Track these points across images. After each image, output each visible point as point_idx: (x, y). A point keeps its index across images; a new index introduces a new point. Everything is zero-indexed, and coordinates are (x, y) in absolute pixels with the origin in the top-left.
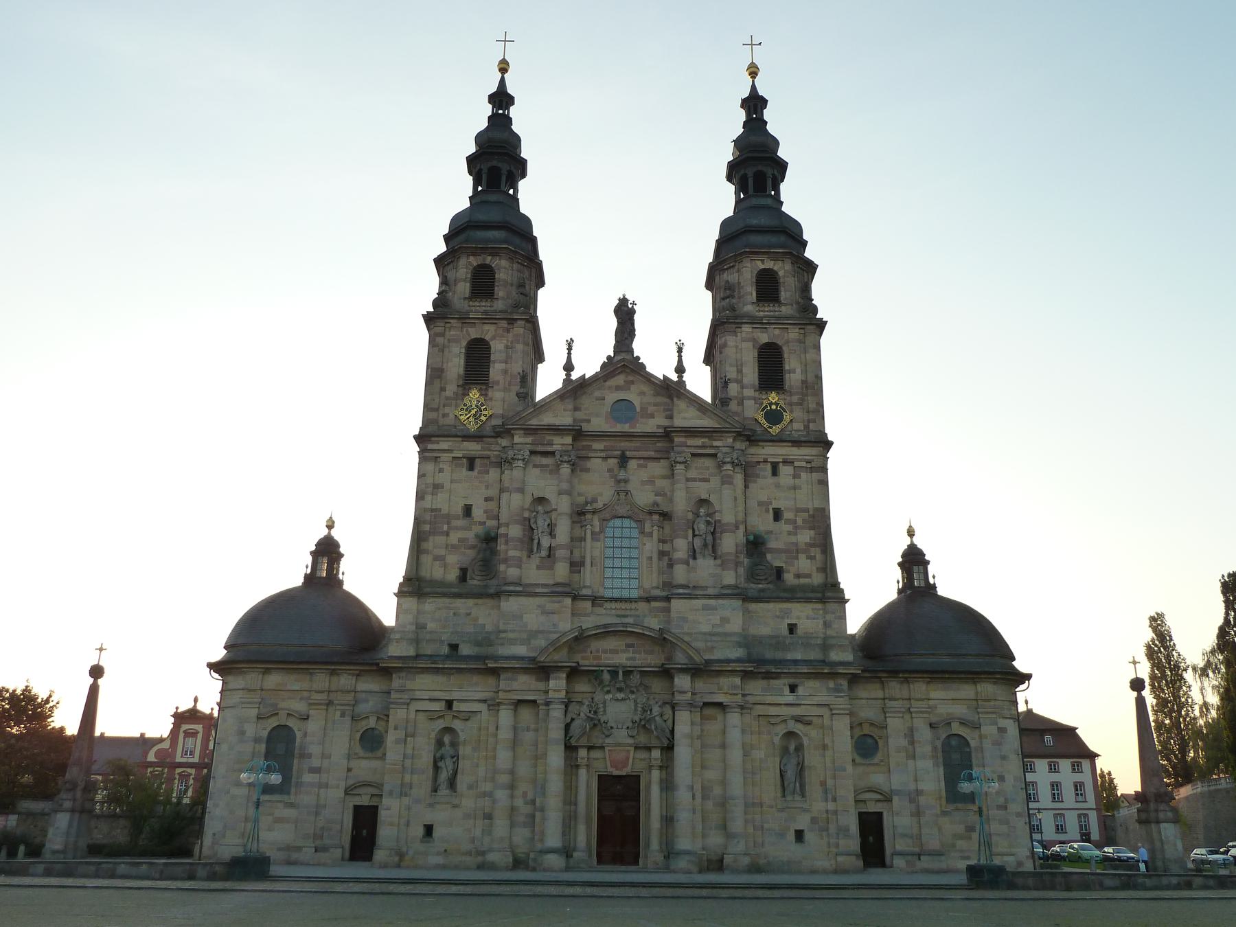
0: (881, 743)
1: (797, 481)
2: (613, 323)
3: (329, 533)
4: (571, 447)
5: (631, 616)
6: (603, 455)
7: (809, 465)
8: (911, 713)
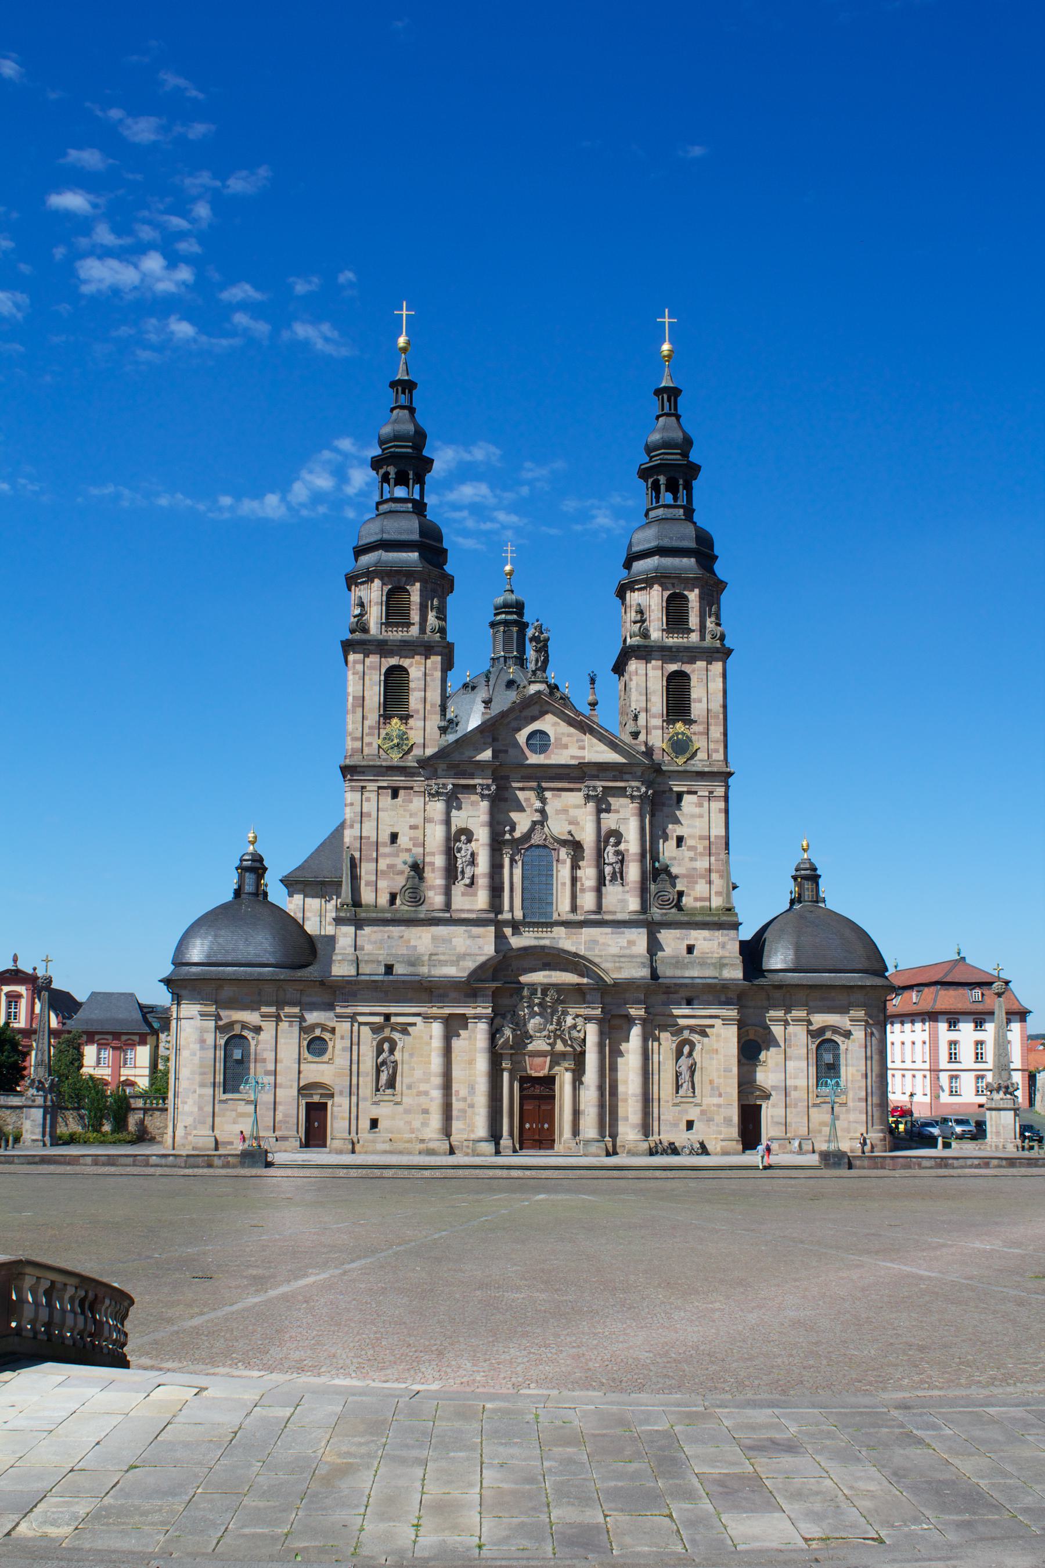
1: (697, 810)
5: (547, 938)
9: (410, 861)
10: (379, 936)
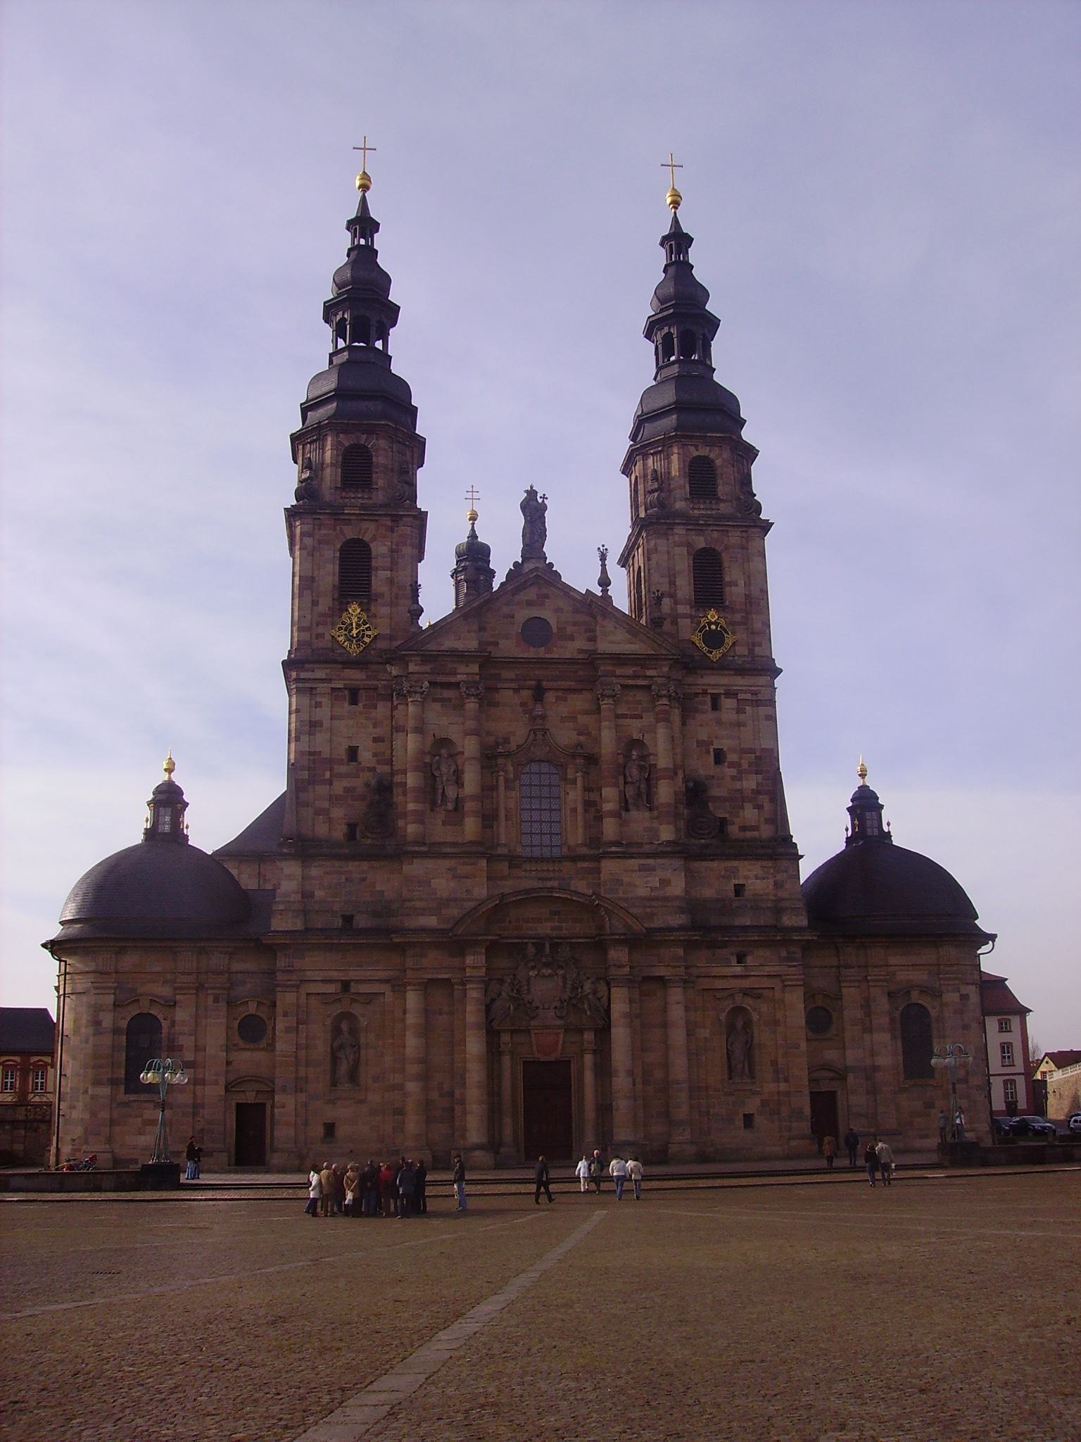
1: (742, 717)
2: (520, 521)
3: (170, 778)
4: (477, 678)
6: (513, 685)
8: (868, 981)
9: (373, 782)
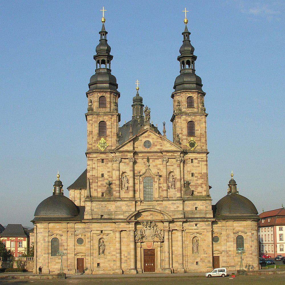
0: (220, 239)
1: (198, 165)
5: (152, 206)
6: (142, 158)
7: (202, 160)
10: (98, 206)
